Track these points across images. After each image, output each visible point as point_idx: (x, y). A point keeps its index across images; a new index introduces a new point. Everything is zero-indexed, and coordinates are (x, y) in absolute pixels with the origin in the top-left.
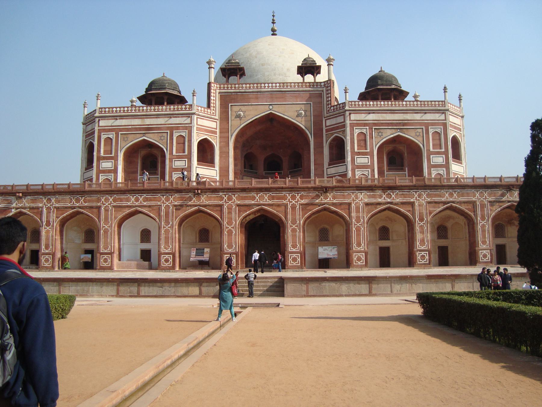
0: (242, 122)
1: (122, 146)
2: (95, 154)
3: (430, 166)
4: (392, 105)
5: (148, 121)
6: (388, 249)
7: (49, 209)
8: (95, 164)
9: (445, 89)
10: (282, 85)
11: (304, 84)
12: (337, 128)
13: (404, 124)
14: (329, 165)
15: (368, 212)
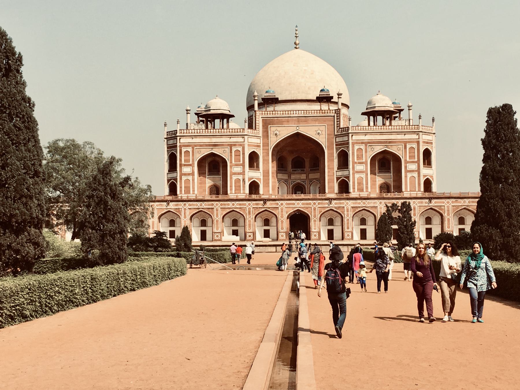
0: (278, 138)
1: (197, 157)
2: (178, 162)
3: (407, 171)
4: (381, 129)
5: (214, 140)
6: (365, 230)
7: (185, 209)
8: (178, 169)
9: (420, 117)
10: (305, 112)
11: (321, 111)
12: (344, 144)
13: (390, 142)
14: (338, 169)
15: (353, 212)
